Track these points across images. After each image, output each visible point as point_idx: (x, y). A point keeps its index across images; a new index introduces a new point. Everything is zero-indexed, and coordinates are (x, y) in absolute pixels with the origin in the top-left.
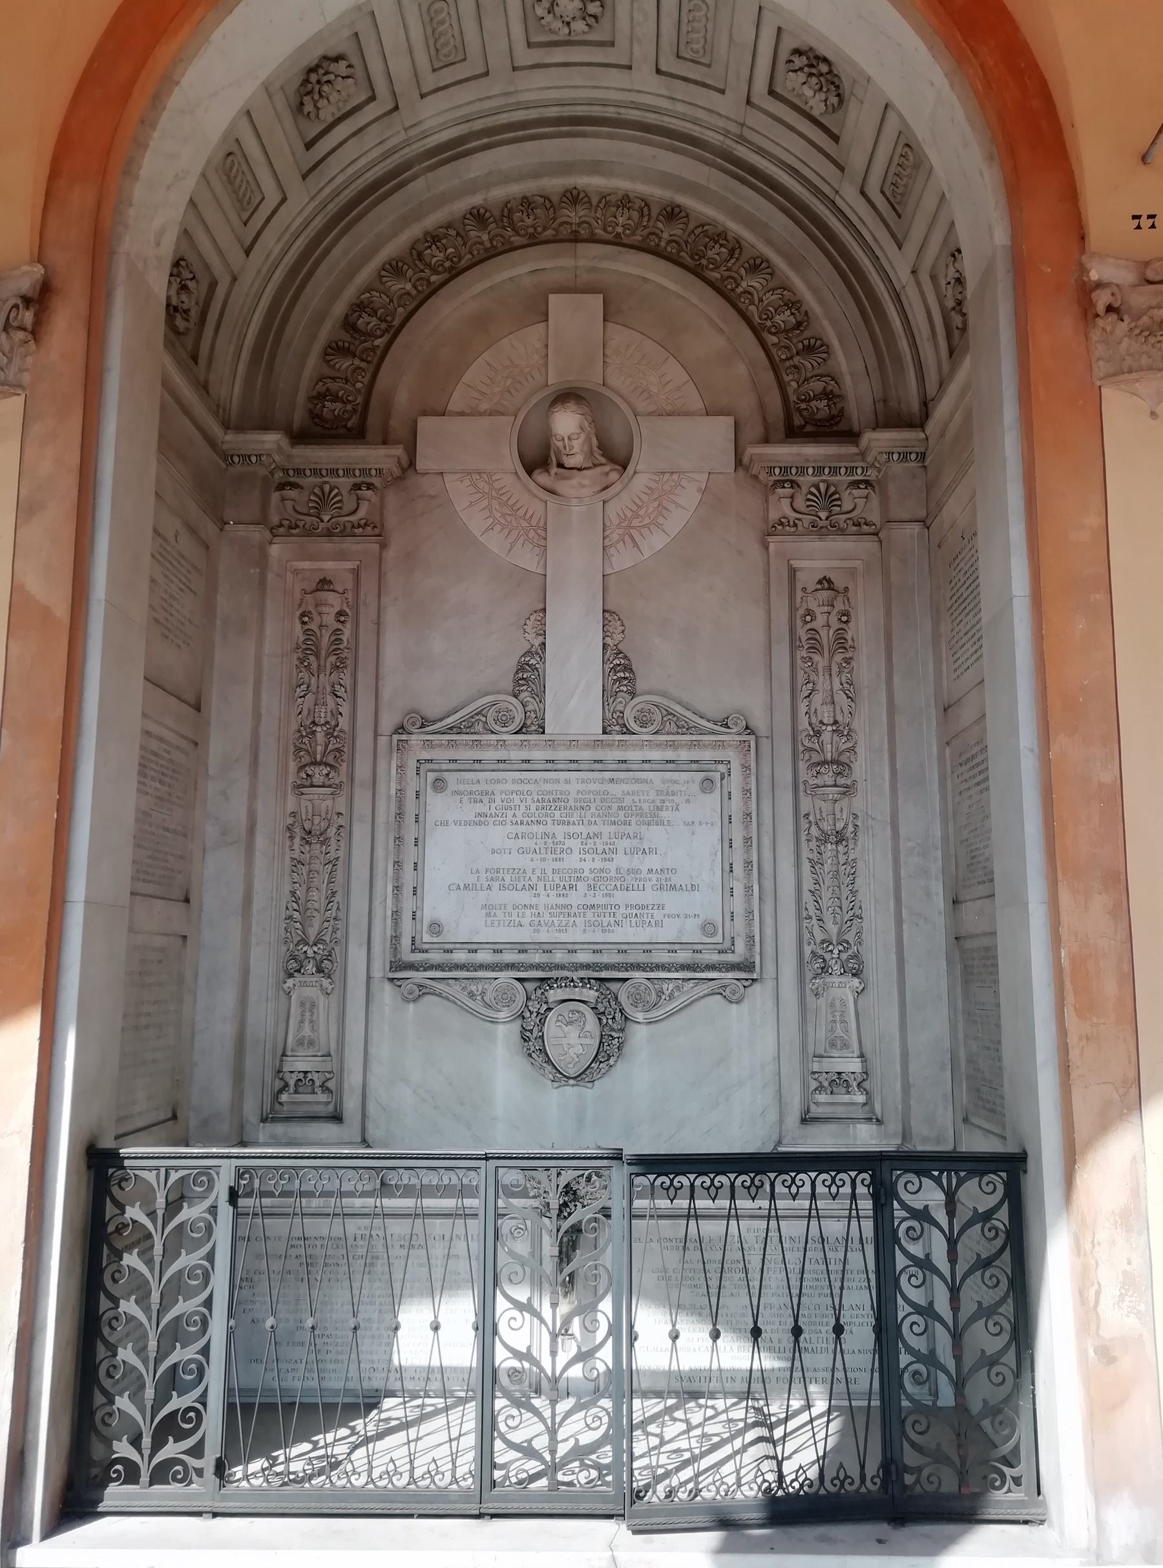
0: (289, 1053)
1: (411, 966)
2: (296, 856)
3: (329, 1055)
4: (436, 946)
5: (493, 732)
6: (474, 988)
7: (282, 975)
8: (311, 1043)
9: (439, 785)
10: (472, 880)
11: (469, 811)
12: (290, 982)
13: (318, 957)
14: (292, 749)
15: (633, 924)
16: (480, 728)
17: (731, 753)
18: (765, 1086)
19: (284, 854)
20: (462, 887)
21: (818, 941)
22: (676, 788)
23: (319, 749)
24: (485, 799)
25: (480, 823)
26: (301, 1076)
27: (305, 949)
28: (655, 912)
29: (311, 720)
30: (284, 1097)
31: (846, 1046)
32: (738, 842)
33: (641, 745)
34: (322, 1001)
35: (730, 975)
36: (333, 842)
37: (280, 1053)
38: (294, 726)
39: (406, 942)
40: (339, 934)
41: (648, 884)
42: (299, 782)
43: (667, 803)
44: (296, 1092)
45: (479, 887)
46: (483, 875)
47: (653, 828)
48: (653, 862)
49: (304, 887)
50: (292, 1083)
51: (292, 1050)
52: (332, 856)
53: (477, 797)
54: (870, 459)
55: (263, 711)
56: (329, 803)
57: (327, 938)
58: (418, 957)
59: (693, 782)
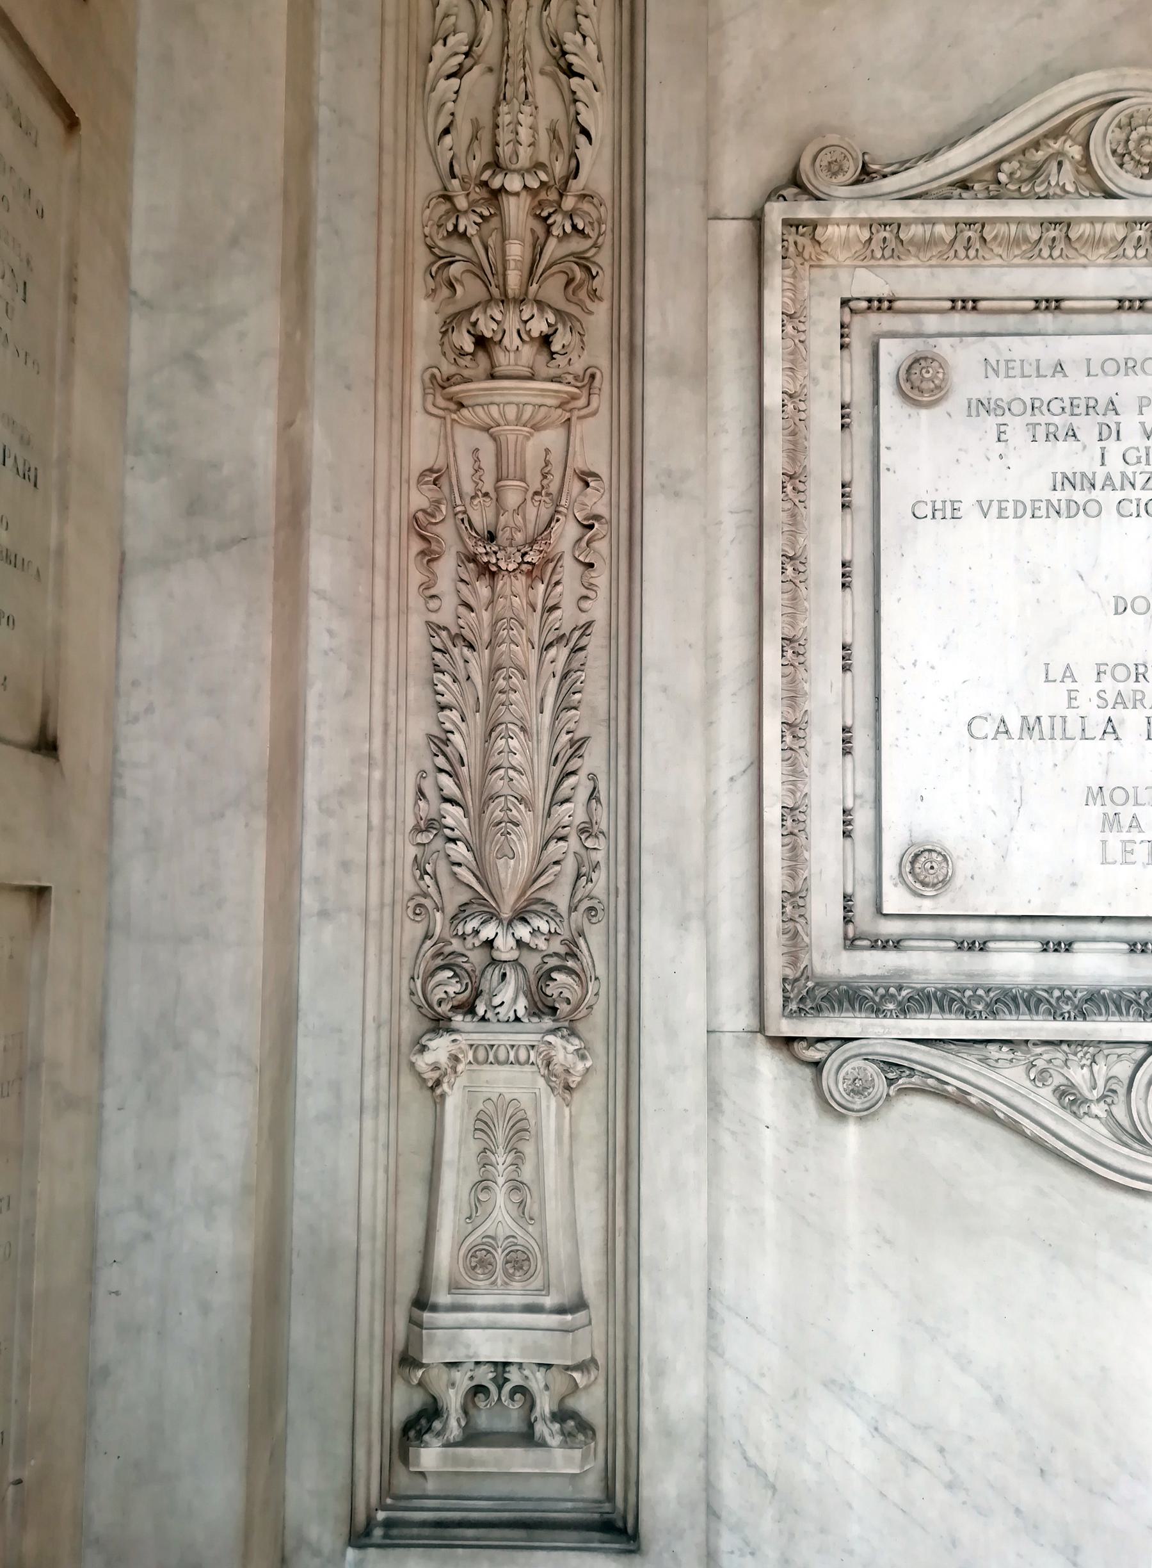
0: (442, 1297)
1: (849, 997)
2: (445, 617)
3: (579, 1305)
4: (927, 927)
5: (1110, 195)
6: (1079, 1076)
7: (409, 1022)
8: (519, 1263)
9: (922, 384)
10: (1049, 701)
11: (1032, 468)
12: (440, 1048)
13: (532, 962)
14: (421, 257)
16: (1067, 177)
19: (404, 611)
20: (1014, 725)
23: (516, 251)
24: (1087, 427)
25: (1072, 510)
26: (485, 1376)
27: (488, 932)
29: (483, 155)
30: (430, 1456)
34: (550, 1114)
36: (569, 570)
37: (407, 1288)
38: (427, 182)
39: (824, 913)
40: (599, 884)
42: (447, 368)
44: (472, 1437)
45: (1074, 728)
46: (1088, 688)
49: (477, 721)
50: (453, 1400)
51: (454, 1287)
52: (566, 618)
53: (1055, 422)
55: (323, 114)
56: (552, 438)
57: (560, 898)
58: (870, 964)
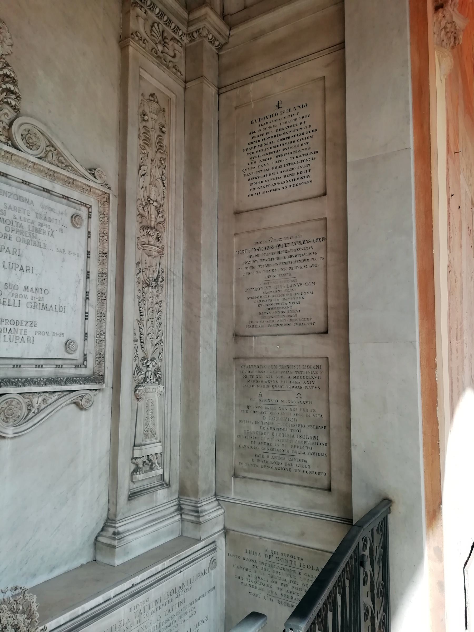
15: (7, 339)
17: (92, 200)
18: (100, 477)
21: (140, 359)
22: (52, 215)
28: (28, 328)
31: (153, 435)
32: (93, 276)
33: (24, 165)
35: (88, 386)
41: (23, 301)
43: (44, 228)
47: (31, 247)
48: (27, 280)
54: (192, 29)
59: (66, 214)
